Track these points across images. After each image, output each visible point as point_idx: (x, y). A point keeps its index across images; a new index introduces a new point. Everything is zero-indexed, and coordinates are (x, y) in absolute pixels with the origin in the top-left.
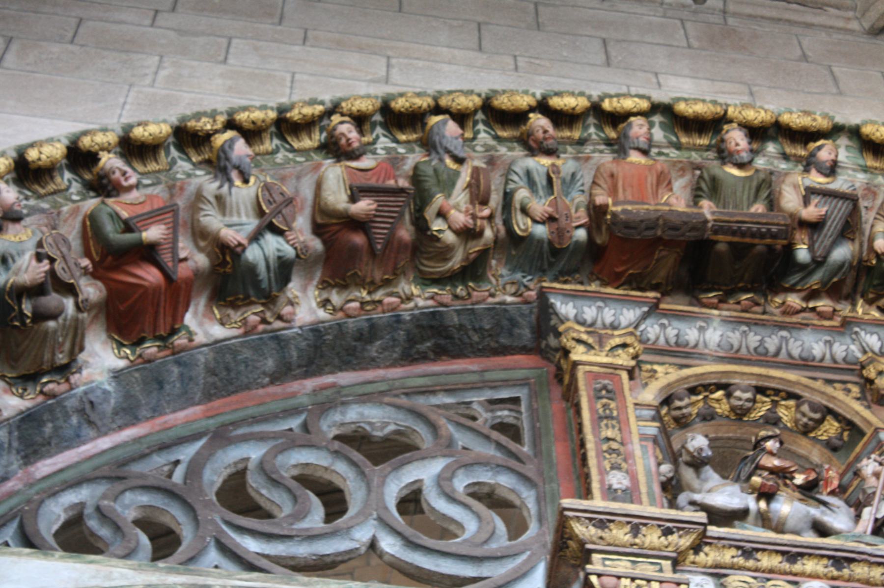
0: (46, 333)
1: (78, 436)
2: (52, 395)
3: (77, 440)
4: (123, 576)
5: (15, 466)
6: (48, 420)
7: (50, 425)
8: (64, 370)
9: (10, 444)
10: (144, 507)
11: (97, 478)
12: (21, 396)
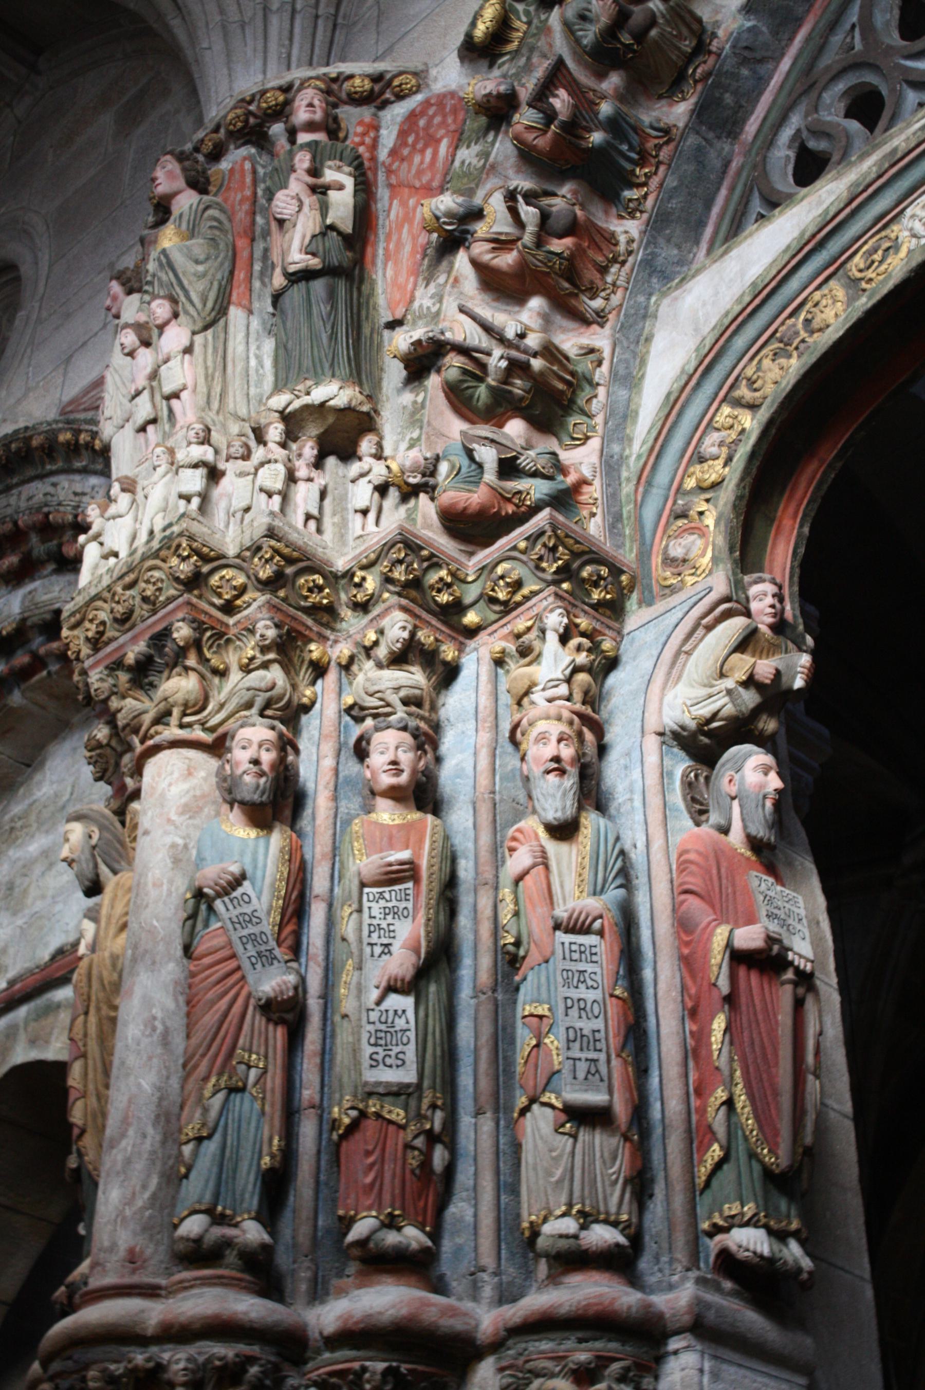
0: (656, 42)
1: (760, 79)
2: (708, 74)
3: (761, 83)
4: (830, 193)
5: (727, 148)
6: (722, 94)
7: (727, 95)
8: (701, 48)
9: (705, 139)
10: (845, 93)
11: (795, 102)
12: (684, 99)
